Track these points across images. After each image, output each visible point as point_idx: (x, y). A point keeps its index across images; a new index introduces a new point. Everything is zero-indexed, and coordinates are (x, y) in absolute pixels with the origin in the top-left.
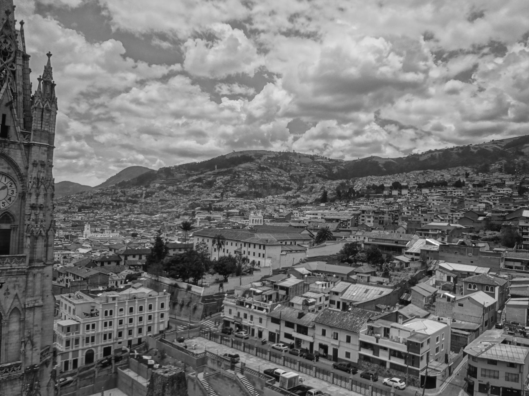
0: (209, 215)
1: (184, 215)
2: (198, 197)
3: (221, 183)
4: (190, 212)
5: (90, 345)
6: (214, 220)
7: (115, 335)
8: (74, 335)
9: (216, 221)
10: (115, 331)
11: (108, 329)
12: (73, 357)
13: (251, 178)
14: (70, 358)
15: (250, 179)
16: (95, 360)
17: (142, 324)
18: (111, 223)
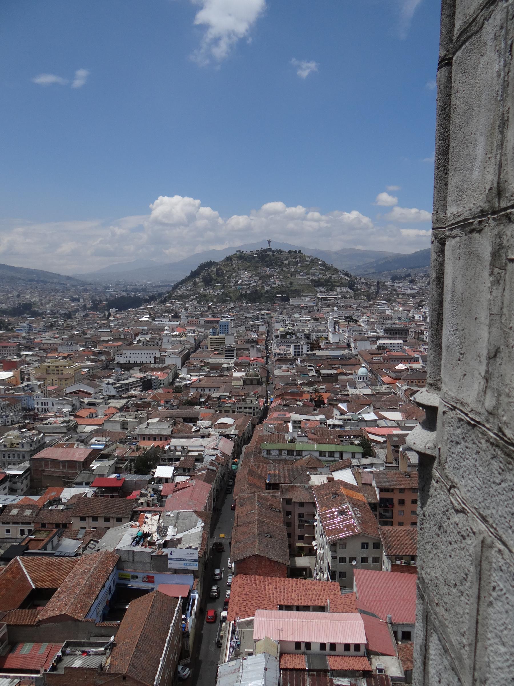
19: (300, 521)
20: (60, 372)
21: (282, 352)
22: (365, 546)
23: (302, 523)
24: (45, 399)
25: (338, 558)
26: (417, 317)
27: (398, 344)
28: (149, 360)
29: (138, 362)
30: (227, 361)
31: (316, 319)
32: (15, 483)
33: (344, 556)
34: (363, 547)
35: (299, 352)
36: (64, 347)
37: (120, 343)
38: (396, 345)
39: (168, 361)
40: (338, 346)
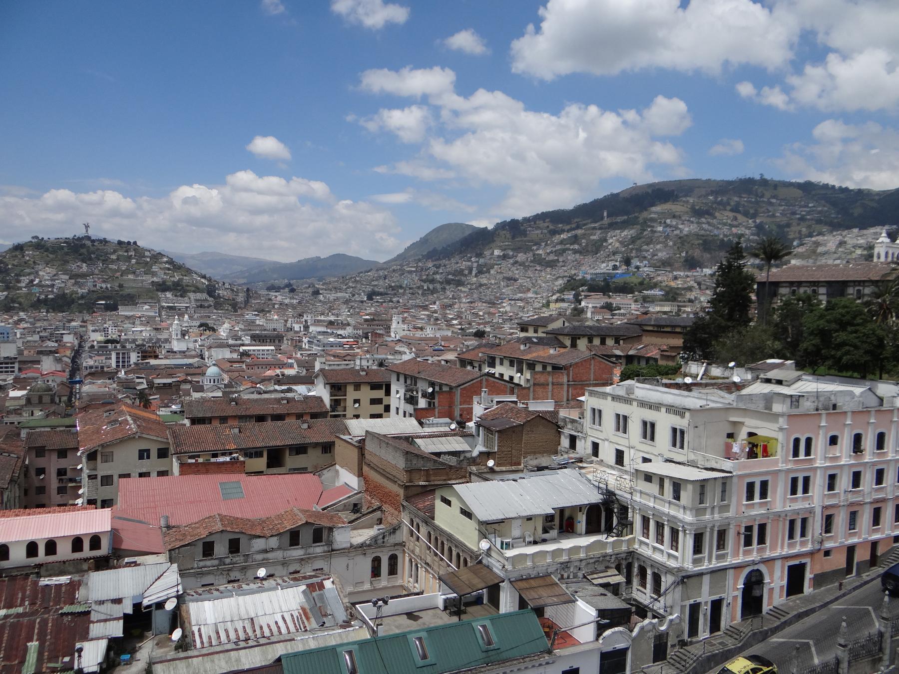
0: (609, 301)
1: (557, 301)
2: (573, 272)
3: (617, 245)
4: (570, 296)
5: (754, 555)
6: (619, 309)
7: (816, 526)
8: (717, 516)
9: (622, 311)
10: (818, 511)
11: (799, 504)
12: (710, 594)
13: (677, 232)
14: (705, 597)
15: (675, 232)
16: (766, 608)
17: (881, 496)
18: (428, 315)
19: (61, 480)
21: (97, 364)
22: (143, 454)
23: (64, 485)
25: (99, 478)
26: (297, 327)
27: (268, 350)
31: (156, 329)
33: (109, 473)
34: (141, 457)
38: (265, 353)
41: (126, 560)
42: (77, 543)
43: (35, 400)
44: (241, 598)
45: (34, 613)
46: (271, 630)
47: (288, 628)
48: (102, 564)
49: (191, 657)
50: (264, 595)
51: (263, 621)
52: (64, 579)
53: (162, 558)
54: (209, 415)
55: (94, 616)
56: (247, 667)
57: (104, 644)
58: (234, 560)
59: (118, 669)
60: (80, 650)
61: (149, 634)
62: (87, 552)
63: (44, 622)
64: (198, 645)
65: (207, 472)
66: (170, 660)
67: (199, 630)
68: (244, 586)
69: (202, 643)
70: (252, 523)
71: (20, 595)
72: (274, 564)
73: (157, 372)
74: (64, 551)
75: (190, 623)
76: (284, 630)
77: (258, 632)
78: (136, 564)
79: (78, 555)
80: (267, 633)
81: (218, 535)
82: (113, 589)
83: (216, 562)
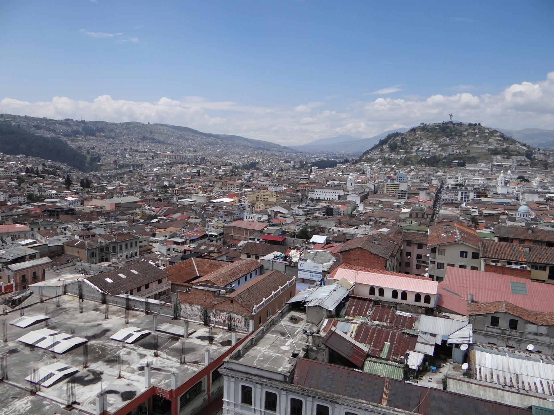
19: (418, 261)
20: (266, 200)
21: (449, 198)
22: (463, 254)
24: (252, 215)
25: (436, 264)
28: (334, 197)
29: (326, 199)
30: (399, 201)
31: (488, 179)
32: (212, 241)
33: (442, 262)
34: (462, 256)
35: (465, 198)
36: (273, 186)
37: (314, 185)
39: (349, 199)
40: (505, 196)
41: (444, 314)
42: (418, 297)
43: (414, 215)
44: (511, 359)
45: (390, 328)
46: (530, 387)
47: (543, 390)
48: (429, 312)
49: (471, 383)
50: (529, 363)
51: (526, 380)
52: (408, 315)
53: (466, 319)
54: (511, 236)
55: (419, 339)
56: (508, 403)
57: (422, 356)
58: (512, 333)
59: (428, 373)
60: (408, 355)
61: (449, 360)
62: (422, 303)
63: (394, 334)
64: (478, 377)
65: (503, 273)
66: (458, 380)
67: (480, 369)
68: (516, 352)
69: (481, 377)
70: (529, 314)
71: (386, 316)
72: (543, 344)
73: (486, 206)
74: (411, 299)
75: (475, 363)
76: (540, 390)
77: (520, 385)
78: (448, 318)
79: (417, 304)
80: (527, 388)
81: (502, 315)
82: (435, 328)
83: (500, 331)
